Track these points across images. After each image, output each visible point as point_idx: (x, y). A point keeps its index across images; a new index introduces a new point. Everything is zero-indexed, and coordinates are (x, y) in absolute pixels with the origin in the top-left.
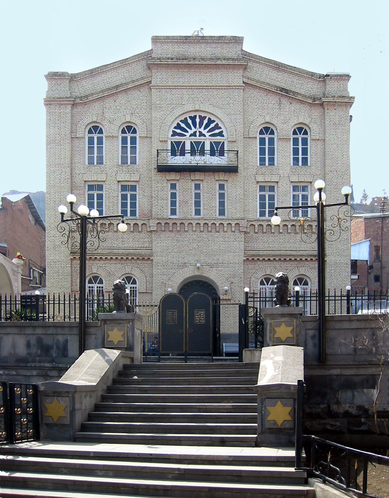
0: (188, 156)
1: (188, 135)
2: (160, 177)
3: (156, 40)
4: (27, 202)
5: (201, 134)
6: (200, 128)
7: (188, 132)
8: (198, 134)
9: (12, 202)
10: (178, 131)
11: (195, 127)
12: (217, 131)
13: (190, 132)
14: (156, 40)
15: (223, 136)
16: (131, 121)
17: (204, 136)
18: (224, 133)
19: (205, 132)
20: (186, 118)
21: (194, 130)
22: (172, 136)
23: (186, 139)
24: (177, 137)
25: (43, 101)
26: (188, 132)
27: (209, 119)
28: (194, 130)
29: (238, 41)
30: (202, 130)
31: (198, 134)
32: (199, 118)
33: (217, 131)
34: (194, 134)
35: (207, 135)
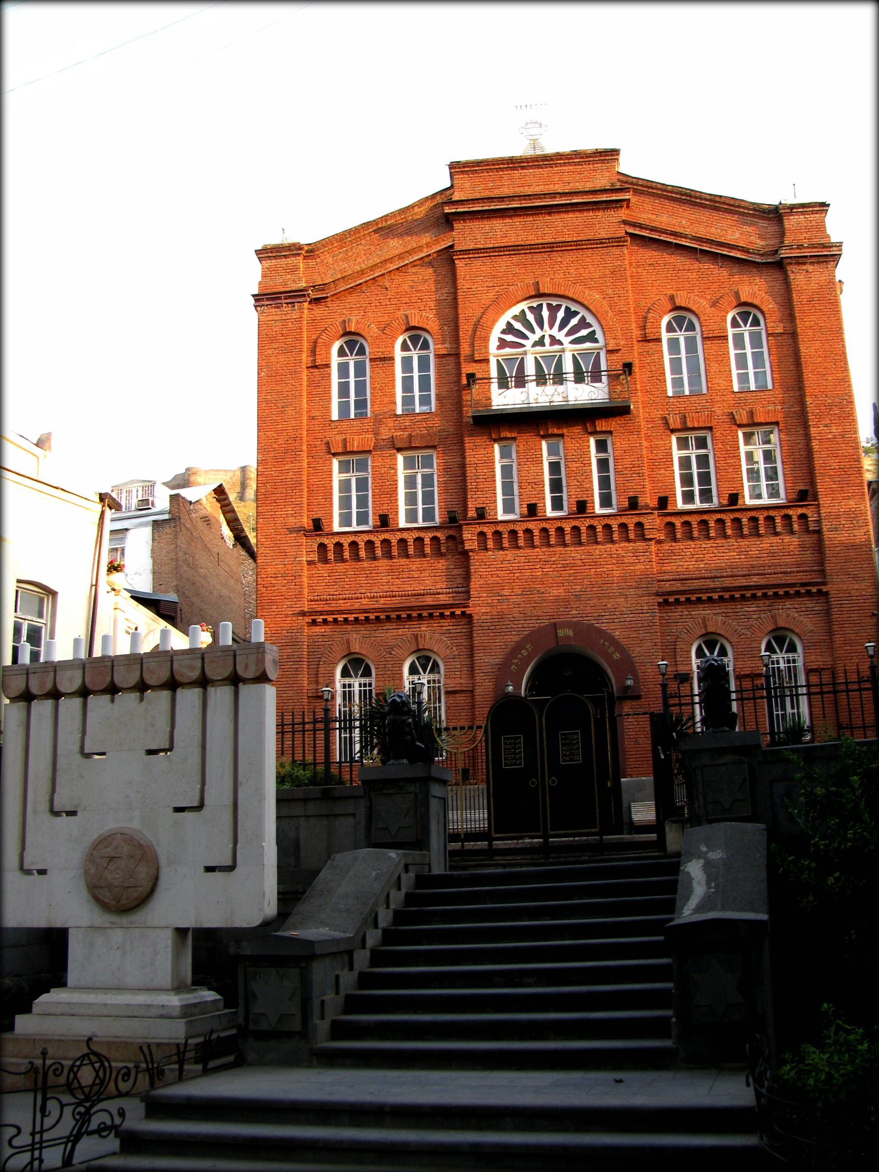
0: (532, 386)
1: (528, 343)
3: (457, 168)
4: (218, 501)
5: (554, 341)
6: (551, 326)
7: (526, 338)
8: (547, 341)
9: (191, 503)
10: (510, 338)
12: (584, 332)
13: (534, 338)
14: (457, 168)
15: (596, 341)
17: (560, 343)
18: (599, 335)
19: (560, 336)
20: (523, 311)
21: (539, 333)
24: (507, 350)
26: (526, 338)
28: (539, 333)
29: (611, 155)
30: (555, 332)
31: (547, 341)
33: (584, 332)
34: (540, 342)
35: (566, 341)
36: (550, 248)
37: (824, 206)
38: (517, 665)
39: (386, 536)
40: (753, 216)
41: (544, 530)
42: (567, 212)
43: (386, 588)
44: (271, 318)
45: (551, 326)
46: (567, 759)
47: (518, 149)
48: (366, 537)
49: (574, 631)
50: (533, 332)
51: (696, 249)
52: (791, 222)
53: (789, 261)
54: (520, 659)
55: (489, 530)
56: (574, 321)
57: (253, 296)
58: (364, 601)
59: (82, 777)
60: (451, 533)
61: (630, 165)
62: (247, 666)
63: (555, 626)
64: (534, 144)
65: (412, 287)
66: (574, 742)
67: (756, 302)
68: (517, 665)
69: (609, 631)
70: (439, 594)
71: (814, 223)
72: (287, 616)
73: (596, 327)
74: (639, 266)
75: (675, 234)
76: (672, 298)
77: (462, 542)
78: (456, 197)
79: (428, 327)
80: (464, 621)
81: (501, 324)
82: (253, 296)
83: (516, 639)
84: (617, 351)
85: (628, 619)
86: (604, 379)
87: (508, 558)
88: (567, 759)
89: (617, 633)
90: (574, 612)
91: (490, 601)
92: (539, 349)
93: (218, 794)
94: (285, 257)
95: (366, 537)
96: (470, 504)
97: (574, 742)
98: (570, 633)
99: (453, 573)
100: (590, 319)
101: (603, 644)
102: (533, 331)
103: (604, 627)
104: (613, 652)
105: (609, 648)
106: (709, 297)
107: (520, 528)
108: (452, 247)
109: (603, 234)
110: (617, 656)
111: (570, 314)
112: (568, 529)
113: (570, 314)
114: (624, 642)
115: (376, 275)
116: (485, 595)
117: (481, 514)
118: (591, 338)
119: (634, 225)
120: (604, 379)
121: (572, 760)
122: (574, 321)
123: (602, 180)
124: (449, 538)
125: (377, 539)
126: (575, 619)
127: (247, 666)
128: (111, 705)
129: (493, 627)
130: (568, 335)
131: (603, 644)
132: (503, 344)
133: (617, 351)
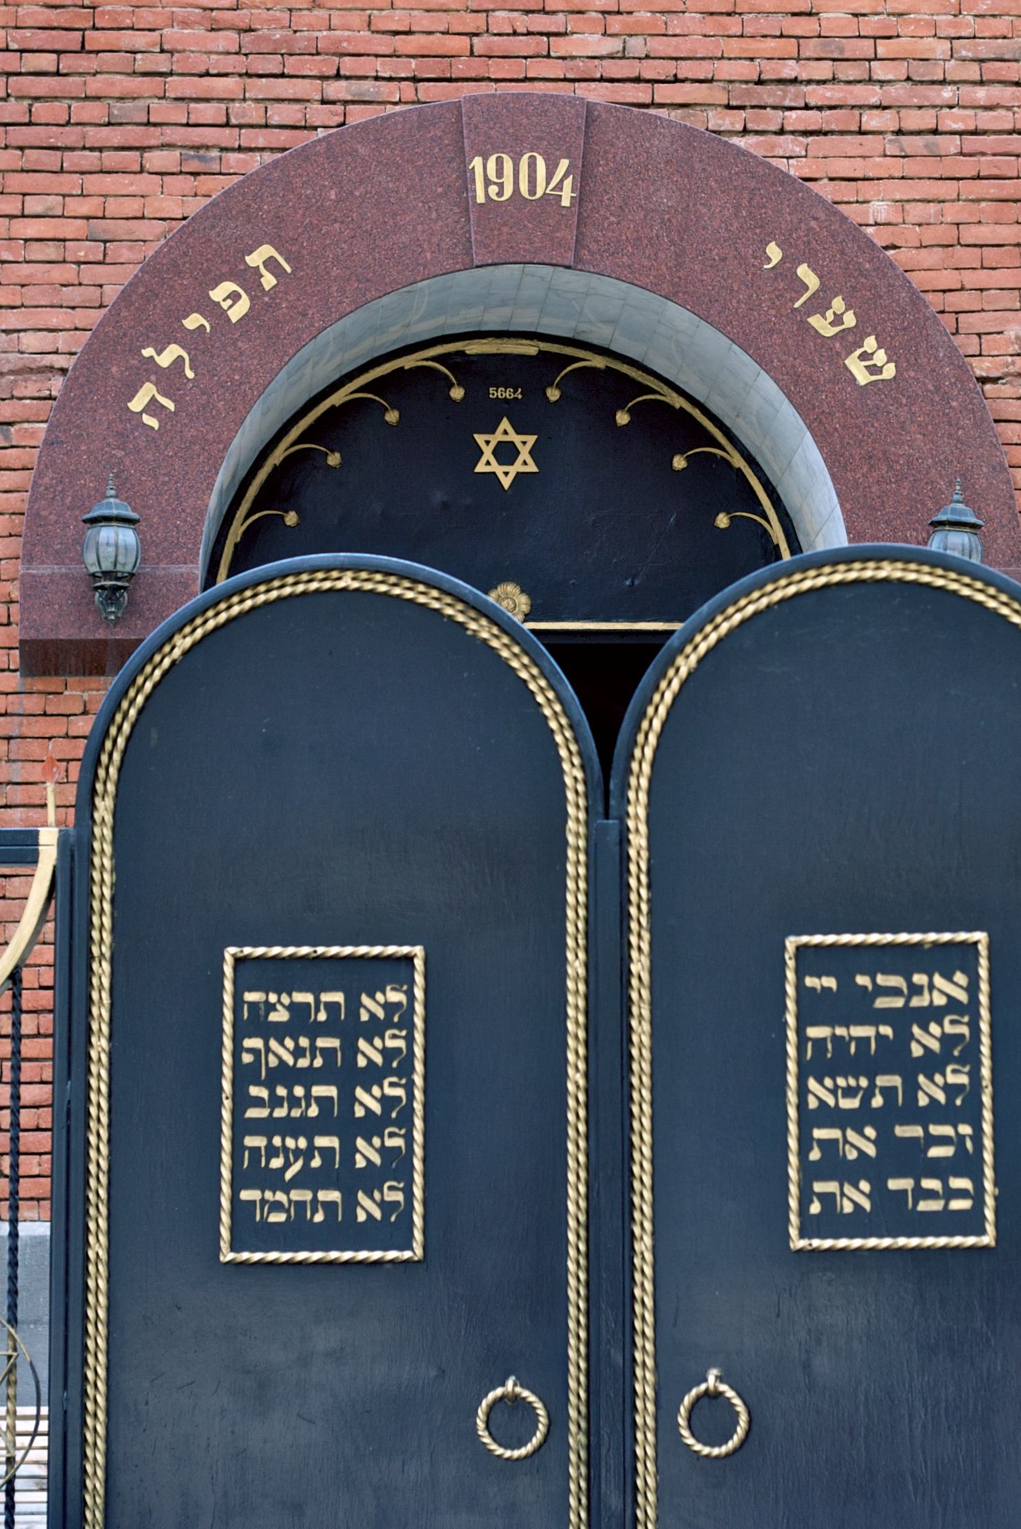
38: (169, 379)
46: (856, 1197)
49: (584, 177)
54: (192, 340)
63: (459, 135)
66: (926, 1040)
68: (169, 379)
69: (826, 191)
83: (179, 201)
85: (953, 120)
88: (856, 1197)
89: (880, 209)
90: (591, 42)
97: (926, 1040)
98: (551, 179)
101: (785, 272)
103: (793, 159)
104: (850, 340)
105: (819, 304)
110: (870, 364)
114: (928, 270)
121: (891, 1213)
126: (596, 94)
131: (785, 272)
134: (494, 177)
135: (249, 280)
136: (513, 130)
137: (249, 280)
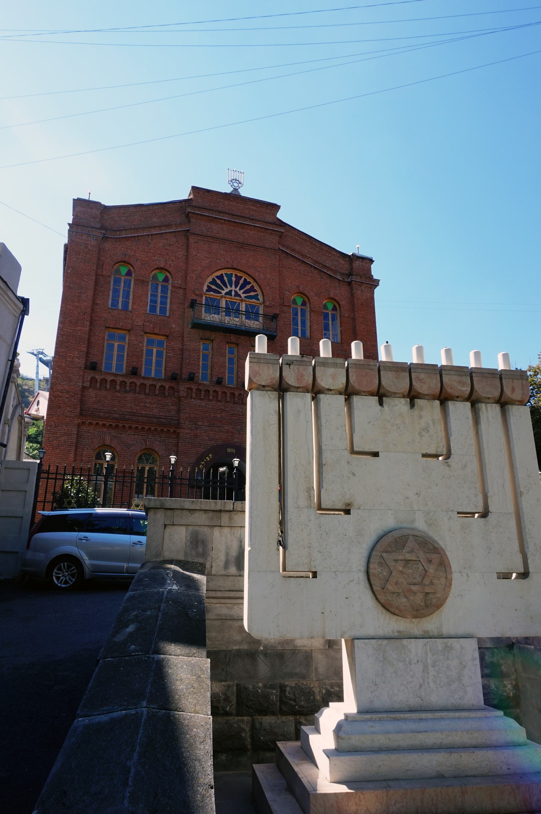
2: (194, 331)
3: (195, 189)
5: (237, 294)
6: (236, 287)
8: (233, 293)
11: (231, 287)
12: (252, 294)
13: (226, 290)
15: (258, 299)
16: (166, 268)
17: (240, 296)
18: (260, 297)
19: (240, 293)
22: (207, 291)
23: (222, 297)
25: (68, 228)
27: (245, 279)
28: (229, 288)
29: (275, 207)
31: (233, 293)
32: (235, 277)
33: (252, 294)
34: (229, 293)
35: (243, 296)
36: (242, 245)
37: (371, 261)
38: (203, 465)
39: (134, 380)
40: (339, 257)
41: (225, 393)
42: (251, 230)
43: (129, 410)
44: (78, 240)
45: (236, 287)
47: (227, 189)
48: (122, 379)
50: (227, 287)
51: (312, 266)
52: (357, 264)
53: (355, 282)
55: (194, 387)
56: (248, 287)
57: (69, 224)
58: (116, 416)
59: (354, 474)
60: (172, 385)
61: (280, 215)
62: (513, 390)
64: (236, 190)
65: (164, 246)
67: (337, 299)
68: (203, 465)
70: (161, 418)
71: (366, 268)
72: (67, 417)
73: (259, 292)
74: (283, 267)
75: (303, 255)
76: (298, 287)
77: (178, 391)
78: (194, 204)
79: (170, 270)
80: (174, 436)
81: (210, 279)
82: (69, 224)
83: (203, 450)
84: (270, 307)
86: (261, 319)
87: (203, 405)
90: (236, 440)
91: (190, 427)
92: (228, 296)
93: (501, 503)
94: (91, 208)
95: (122, 379)
96: (184, 371)
99: (170, 408)
100: (256, 288)
102: (227, 287)
106: (315, 291)
107: (211, 389)
108: (188, 230)
109: (267, 246)
111: (246, 283)
112: (237, 394)
113: (246, 283)
115: (145, 234)
116: (187, 423)
117: (191, 378)
118: (256, 297)
119: (283, 246)
120: (261, 319)
122: (248, 287)
123: (270, 219)
124: (171, 388)
125: (128, 381)
127: (513, 390)
128: (379, 407)
129: (190, 442)
130: (243, 293)
132: (209, 289)
133: (270, 307)
134: (229, 450)
135: (209, 457)
136: (231, 446)
137: (209, 457)
